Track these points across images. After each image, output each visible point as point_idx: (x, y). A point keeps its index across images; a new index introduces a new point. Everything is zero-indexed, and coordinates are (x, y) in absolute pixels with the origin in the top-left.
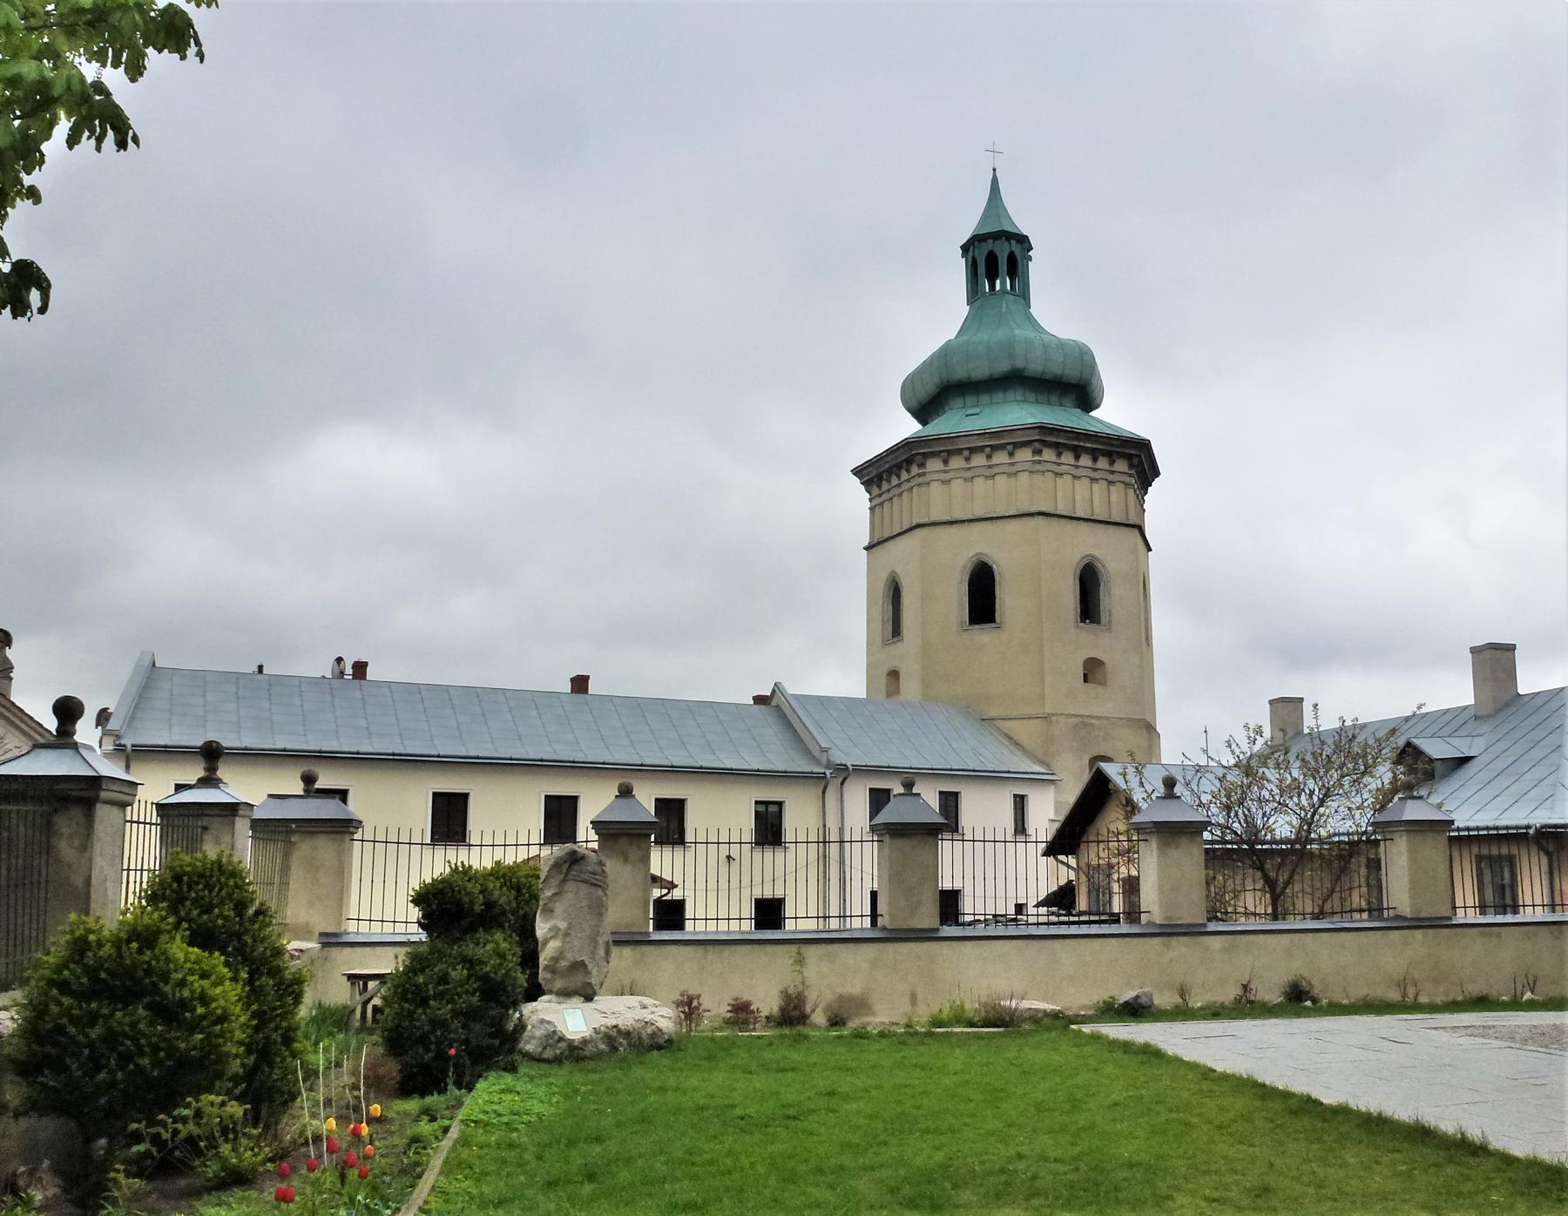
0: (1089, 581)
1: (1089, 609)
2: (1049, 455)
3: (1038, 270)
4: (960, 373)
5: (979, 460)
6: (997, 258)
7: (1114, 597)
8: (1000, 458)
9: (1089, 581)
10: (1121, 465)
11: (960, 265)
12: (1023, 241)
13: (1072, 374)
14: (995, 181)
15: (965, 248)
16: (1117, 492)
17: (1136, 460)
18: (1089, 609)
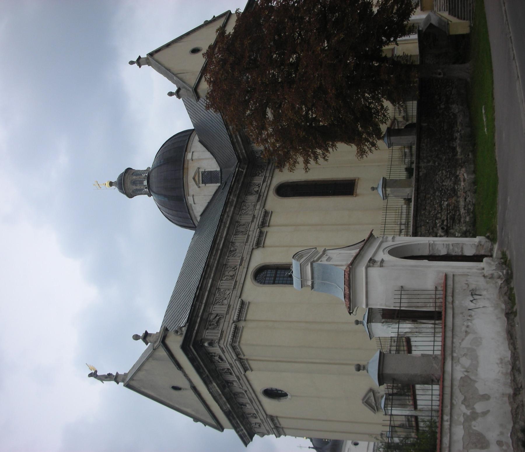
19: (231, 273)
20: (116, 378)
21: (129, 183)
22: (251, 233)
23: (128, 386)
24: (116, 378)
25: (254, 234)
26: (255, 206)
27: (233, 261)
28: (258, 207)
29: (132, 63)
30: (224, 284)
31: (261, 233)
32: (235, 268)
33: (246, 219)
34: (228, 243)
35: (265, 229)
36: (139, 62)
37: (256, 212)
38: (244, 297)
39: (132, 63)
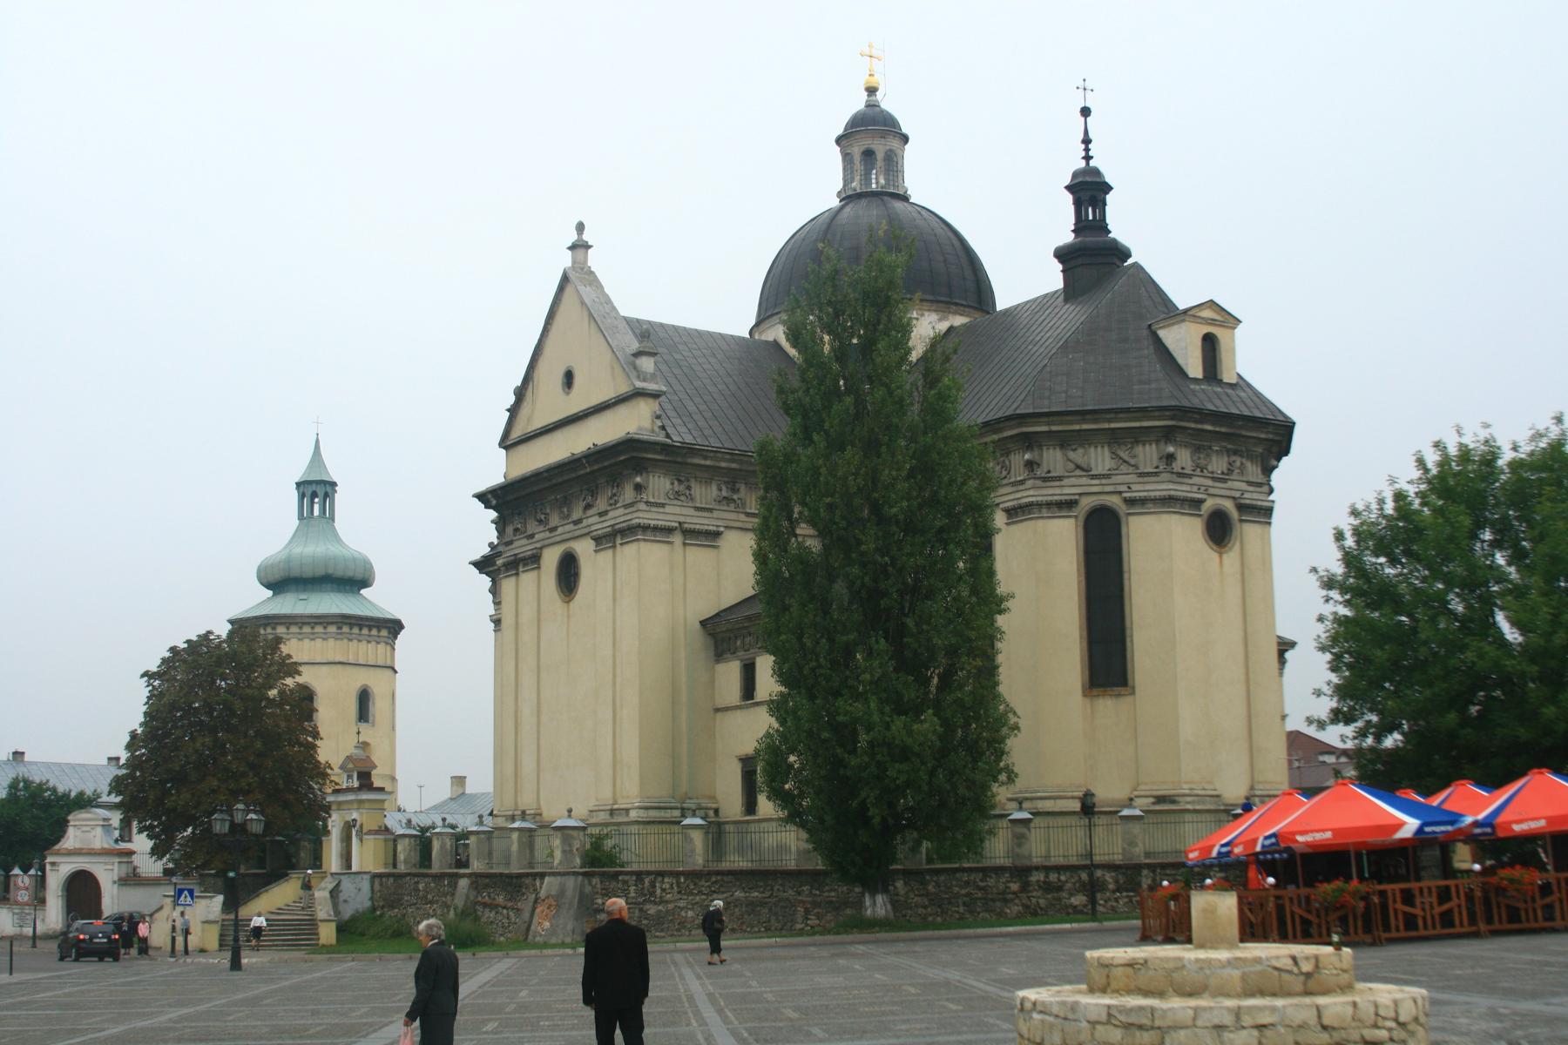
0: (364, 698)
1: (363, 714)
2: (346, 629)
3: (340, 497)
4: (295, 573)
5: (307, 629)
6: (316, 492)
7: (378, 707)
8: (319, 629)
9: (364, 698)
10: (384, 633)
11: (295, 495)
12: (334, 484)
13: (359, 576)
14: (317, 441)
15: (298, 485)
16: (381, 647)
17: (394, 627)
18: (363, 714)
21: (872, 138)
29: (580, 227)
36: (580, 247)
39: (580, 227)
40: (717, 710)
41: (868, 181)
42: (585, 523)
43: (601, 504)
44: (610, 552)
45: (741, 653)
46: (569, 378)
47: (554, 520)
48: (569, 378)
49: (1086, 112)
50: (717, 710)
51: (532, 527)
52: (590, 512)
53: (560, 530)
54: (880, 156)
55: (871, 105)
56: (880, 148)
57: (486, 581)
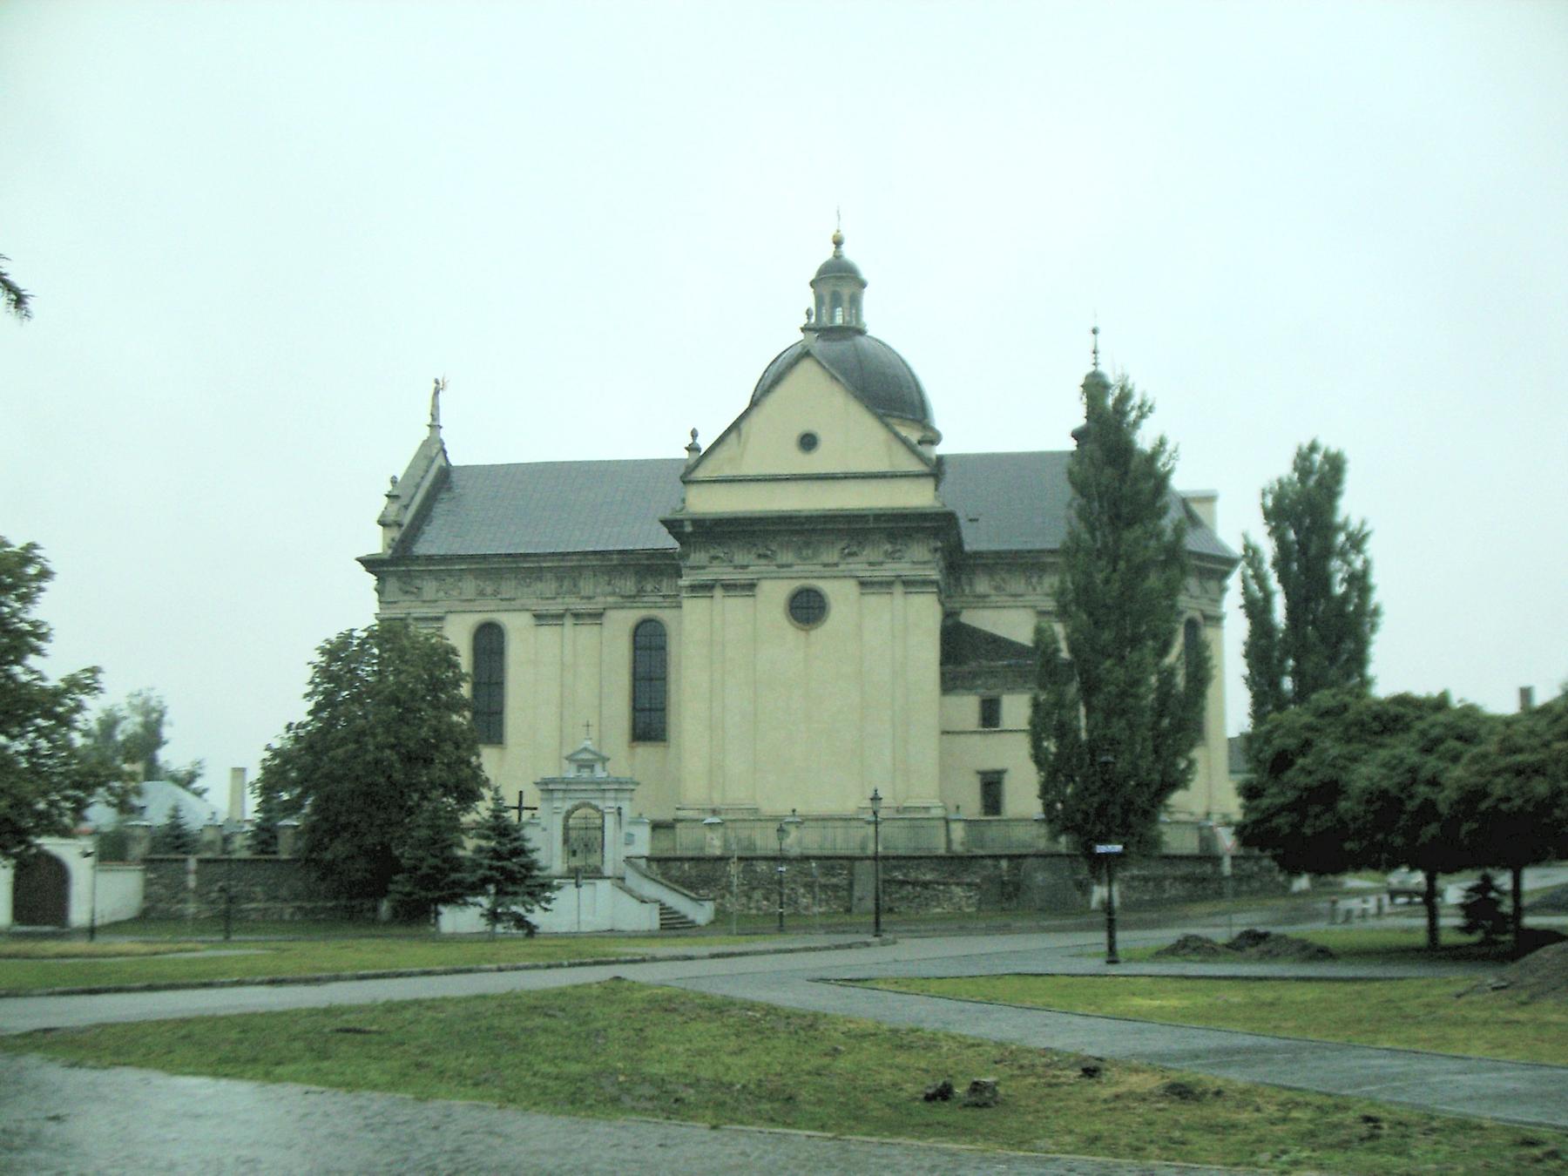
19: (489, 590)
20: (435, 426)
21: (838, 281)
22: (559, 600)
23: (426, 444)
24: (435, 426)
25: (555, 607)
26: (613, 594)
27: (508, 587)
28: (610, 599)
30: (469, 586)
31: (560, 616)
32: (496, 593)
33: (587, 586)
34: (537, 574)
35: (569, 621)
37: (601, 599)
38: (450, 617)
40: (945, 733)
41: (832, 317)
42: (842, 567)
43: (869, 554)
44: (885, 599)
45: (982, 691)
46: (808, 442)
47: (786, 557)
48: (808, 442)
49: (1095, 331)
50: (945, 733)
51: (740, 558)
52: (850, 560)
53: (796, 568)
54: (846, 298)
55: (837, 256)
56: (846, 292)
57: (372, 580)
